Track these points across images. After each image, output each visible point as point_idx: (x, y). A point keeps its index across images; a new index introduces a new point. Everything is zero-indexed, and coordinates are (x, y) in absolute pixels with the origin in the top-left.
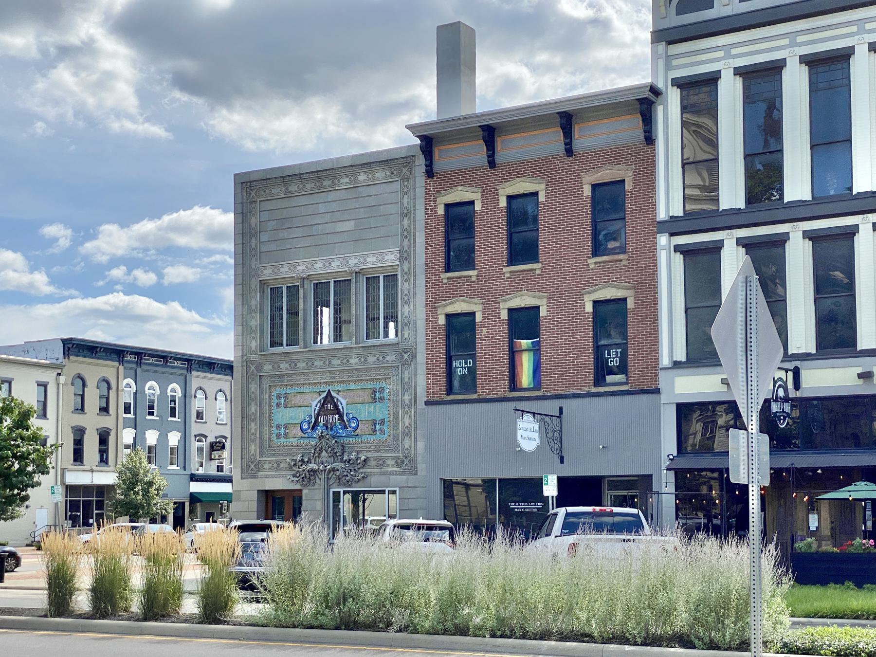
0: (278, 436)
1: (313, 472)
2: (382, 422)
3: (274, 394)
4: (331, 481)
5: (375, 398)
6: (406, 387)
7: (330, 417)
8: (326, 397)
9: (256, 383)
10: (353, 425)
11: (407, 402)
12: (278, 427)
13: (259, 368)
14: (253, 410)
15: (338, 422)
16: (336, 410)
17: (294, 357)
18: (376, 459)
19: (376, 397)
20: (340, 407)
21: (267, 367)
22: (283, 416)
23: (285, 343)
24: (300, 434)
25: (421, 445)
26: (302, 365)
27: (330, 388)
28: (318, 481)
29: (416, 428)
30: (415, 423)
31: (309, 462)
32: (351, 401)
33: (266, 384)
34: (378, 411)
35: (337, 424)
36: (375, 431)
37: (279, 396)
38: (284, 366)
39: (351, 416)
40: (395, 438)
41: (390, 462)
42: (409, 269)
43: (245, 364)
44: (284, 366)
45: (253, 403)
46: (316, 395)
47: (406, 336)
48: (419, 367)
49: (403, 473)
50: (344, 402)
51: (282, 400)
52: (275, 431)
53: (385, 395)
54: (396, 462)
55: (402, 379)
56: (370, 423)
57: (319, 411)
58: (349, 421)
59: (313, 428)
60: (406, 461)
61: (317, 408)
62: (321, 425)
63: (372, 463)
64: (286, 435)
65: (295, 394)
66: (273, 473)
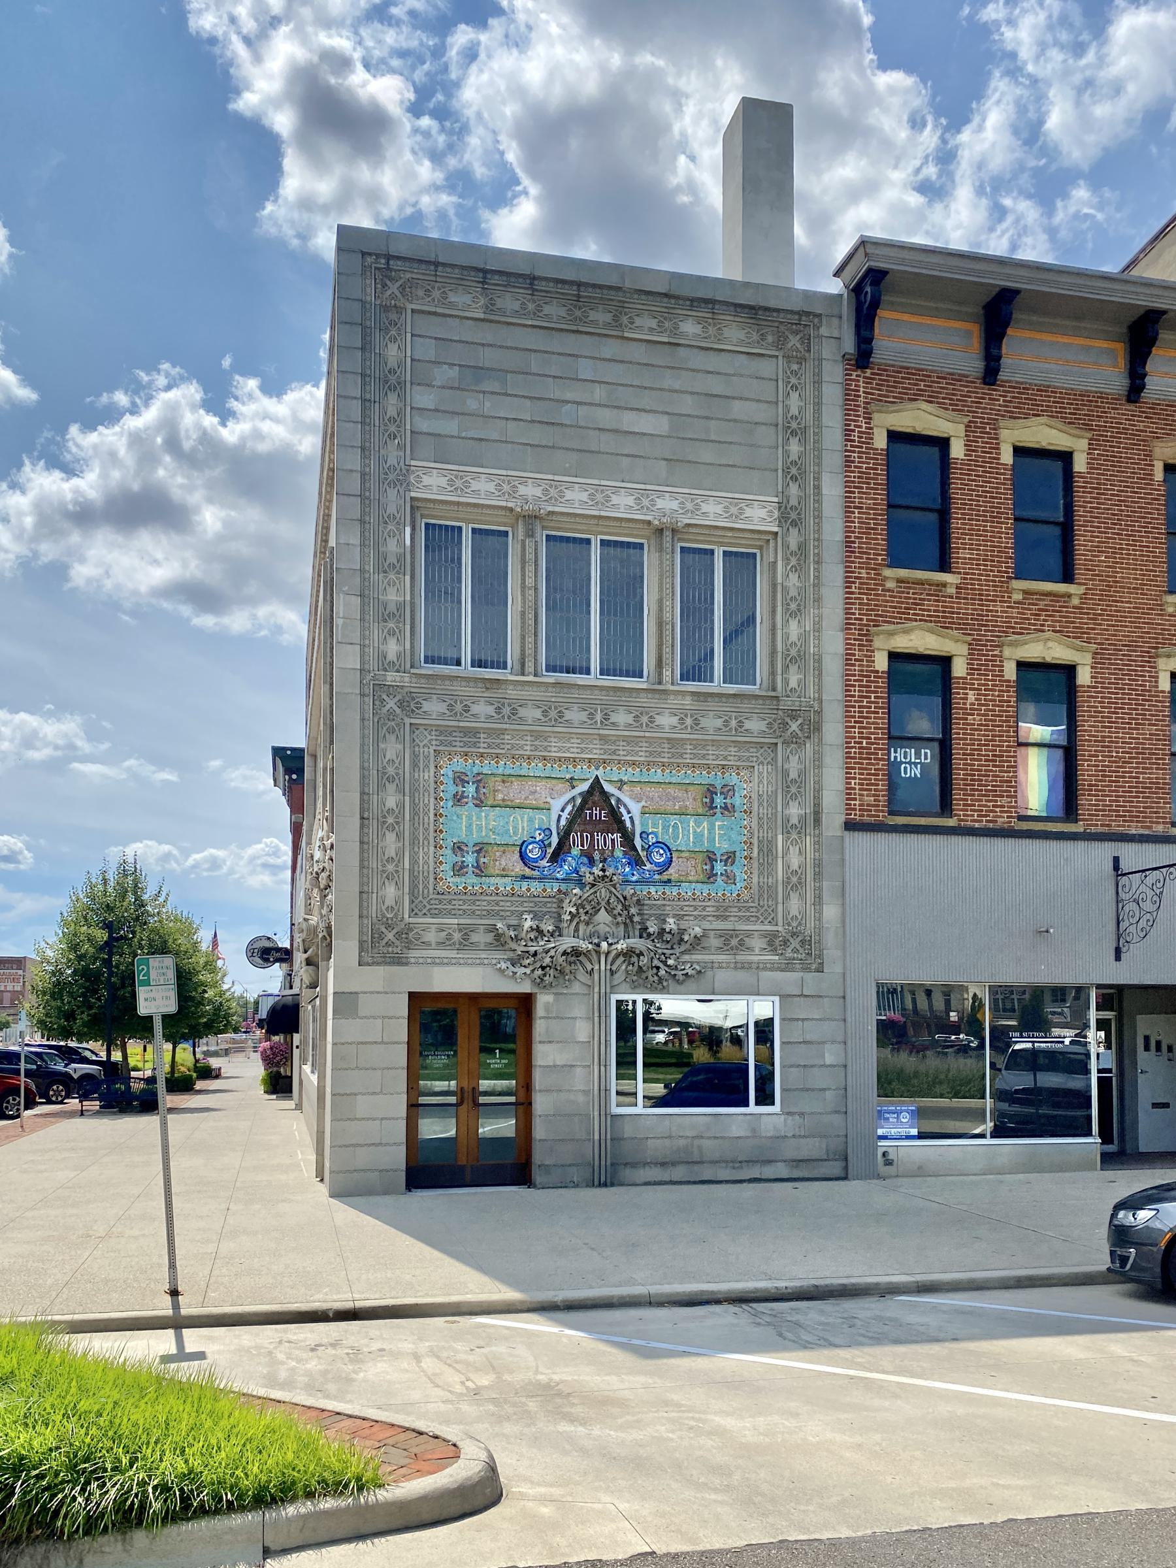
0: (459, 869)
1: (575, 954)
2: (730, 858)
3: (447, 771)
4: (620, 977)
5: (711, 807)
6: (793, 790)
7: (599, 837)
8: (590, 792)
9: (400, 740)
11: (794, 820)
12: (458, 848)
13: (410, 704)
14: (391, 802)
15: (618, 853)
16: (615, 821)
17: (512, 693)
18: (726, 937)
19: (713, 802)
20: (626, 817)
21: (434, 707)
22: (470, 824)
23: (467, 656)
24: (519, 868)
25: (830, 912)
26: (531, 713)
27: (600, 773)
28: (582, 976)
29: (818, 876)
30: (818, 864)
31: (558, 932)
33: (428, 744)
34: (718, 834)
36: (711, 876)
37: (460, 779)
38: (482, 709)
39: (652, 839)
40: (767, 891)
41: (758, 943)
43: (369, 690)
44: (482, 709)
45: (391, 788)
47: (793, 683)
48: (826, 749)
49: (787, 967)
50: (635, 808)
51: (471, 789)
52: (449, 858)
53: (737, 801)
55: (785, 773)
56: (701, 857)
57: (571, 823)
58: (648, 849)
59: (557, 856)
60: (795, 943)
61: (565, 815)
62: (575, 851)
63: (714, 942)
64: (480, 870)
65: (506, 779)
66: (453, 954)
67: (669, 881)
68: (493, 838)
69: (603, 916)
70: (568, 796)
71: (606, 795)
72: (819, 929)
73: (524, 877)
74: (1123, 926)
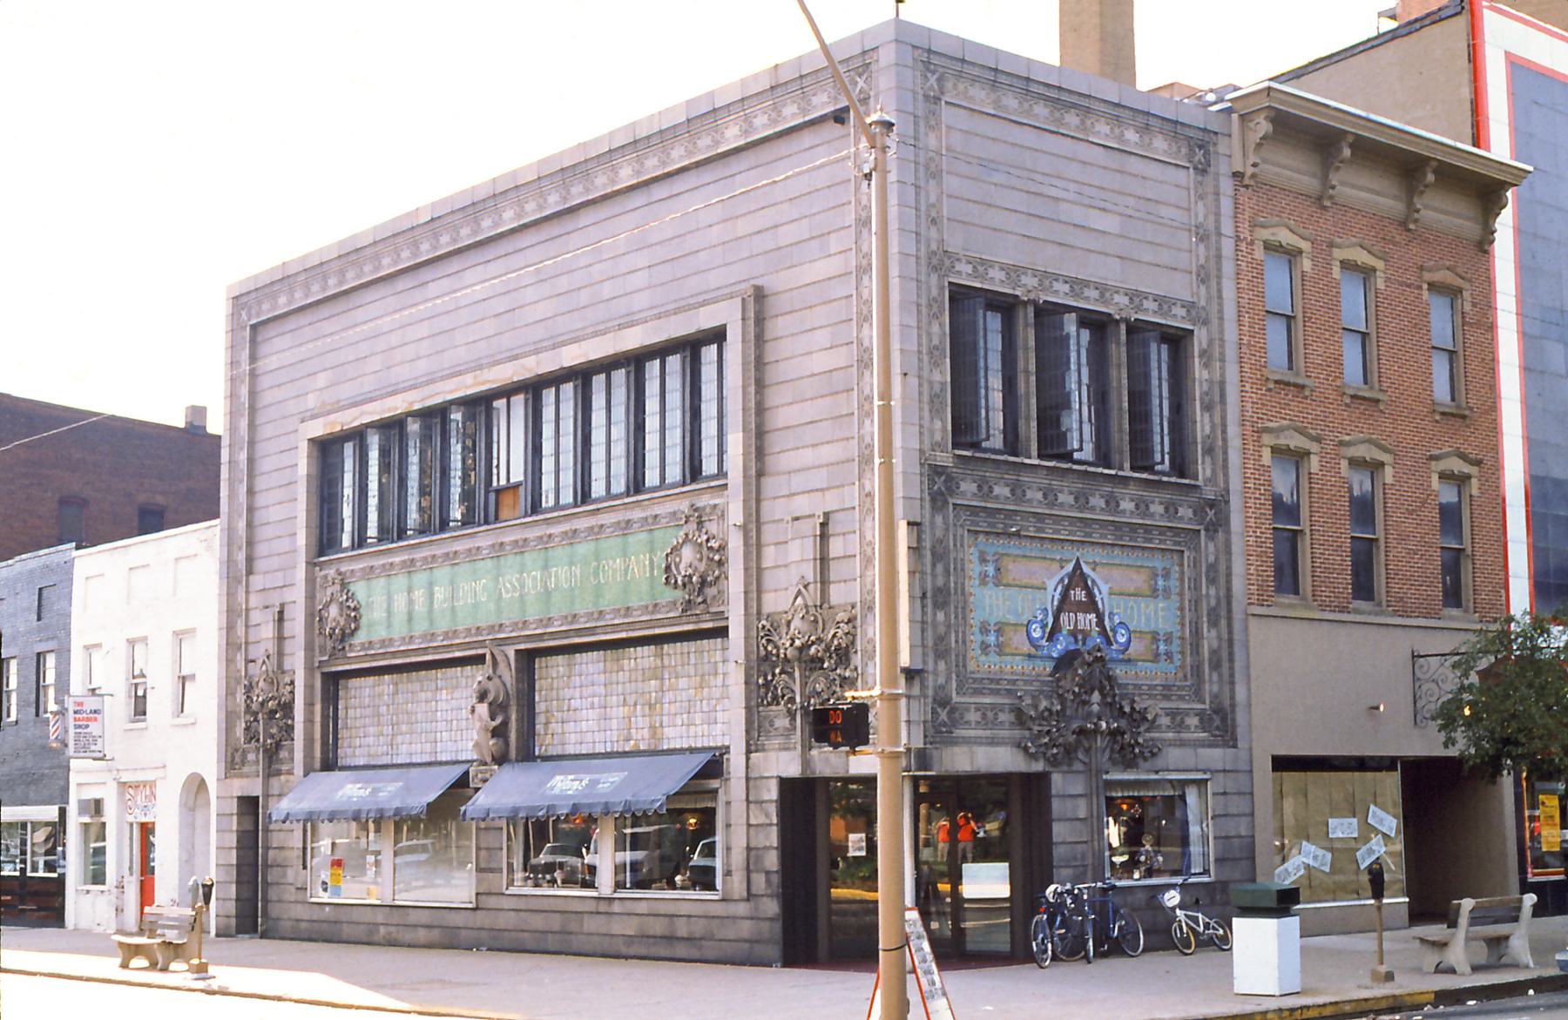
7: (1080, 616)
10: (1122, 640)
16: (1091, 605)
20: (1098, 599)
24: (1026, 648)
32: (1117, 589)
35: (1094, 634)
38: (1001, 490)
42: (1211, 342)
46: (1056, 566)
50: (1105, 588)
54: (1201, 721)
61: (1057, 597)
64: (1001, 649)
67: (1129, 660)
68: (1011, 619)
69: (1096, 697)
70: (1058, 578)
71: (1084, 577)
72: (1233, 706)
73: (1030, 656)
74: (1419, 705)
